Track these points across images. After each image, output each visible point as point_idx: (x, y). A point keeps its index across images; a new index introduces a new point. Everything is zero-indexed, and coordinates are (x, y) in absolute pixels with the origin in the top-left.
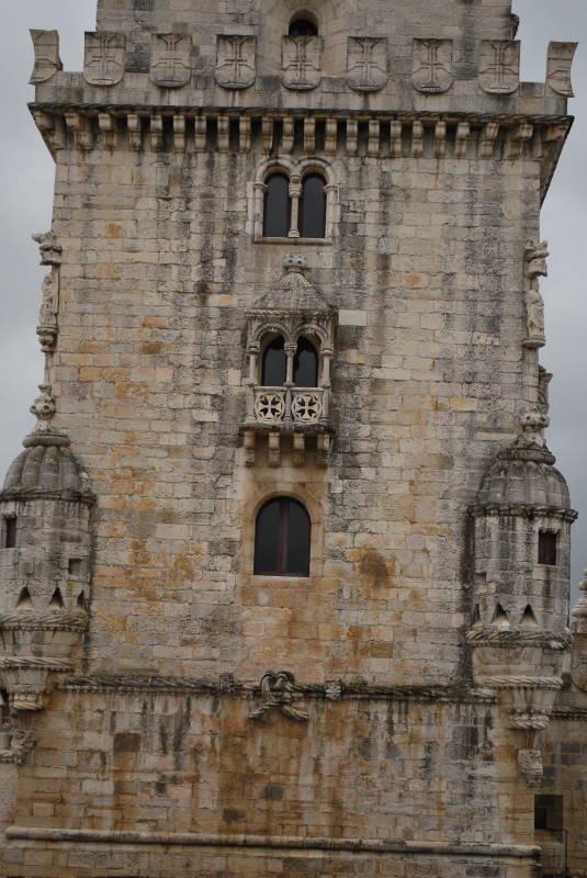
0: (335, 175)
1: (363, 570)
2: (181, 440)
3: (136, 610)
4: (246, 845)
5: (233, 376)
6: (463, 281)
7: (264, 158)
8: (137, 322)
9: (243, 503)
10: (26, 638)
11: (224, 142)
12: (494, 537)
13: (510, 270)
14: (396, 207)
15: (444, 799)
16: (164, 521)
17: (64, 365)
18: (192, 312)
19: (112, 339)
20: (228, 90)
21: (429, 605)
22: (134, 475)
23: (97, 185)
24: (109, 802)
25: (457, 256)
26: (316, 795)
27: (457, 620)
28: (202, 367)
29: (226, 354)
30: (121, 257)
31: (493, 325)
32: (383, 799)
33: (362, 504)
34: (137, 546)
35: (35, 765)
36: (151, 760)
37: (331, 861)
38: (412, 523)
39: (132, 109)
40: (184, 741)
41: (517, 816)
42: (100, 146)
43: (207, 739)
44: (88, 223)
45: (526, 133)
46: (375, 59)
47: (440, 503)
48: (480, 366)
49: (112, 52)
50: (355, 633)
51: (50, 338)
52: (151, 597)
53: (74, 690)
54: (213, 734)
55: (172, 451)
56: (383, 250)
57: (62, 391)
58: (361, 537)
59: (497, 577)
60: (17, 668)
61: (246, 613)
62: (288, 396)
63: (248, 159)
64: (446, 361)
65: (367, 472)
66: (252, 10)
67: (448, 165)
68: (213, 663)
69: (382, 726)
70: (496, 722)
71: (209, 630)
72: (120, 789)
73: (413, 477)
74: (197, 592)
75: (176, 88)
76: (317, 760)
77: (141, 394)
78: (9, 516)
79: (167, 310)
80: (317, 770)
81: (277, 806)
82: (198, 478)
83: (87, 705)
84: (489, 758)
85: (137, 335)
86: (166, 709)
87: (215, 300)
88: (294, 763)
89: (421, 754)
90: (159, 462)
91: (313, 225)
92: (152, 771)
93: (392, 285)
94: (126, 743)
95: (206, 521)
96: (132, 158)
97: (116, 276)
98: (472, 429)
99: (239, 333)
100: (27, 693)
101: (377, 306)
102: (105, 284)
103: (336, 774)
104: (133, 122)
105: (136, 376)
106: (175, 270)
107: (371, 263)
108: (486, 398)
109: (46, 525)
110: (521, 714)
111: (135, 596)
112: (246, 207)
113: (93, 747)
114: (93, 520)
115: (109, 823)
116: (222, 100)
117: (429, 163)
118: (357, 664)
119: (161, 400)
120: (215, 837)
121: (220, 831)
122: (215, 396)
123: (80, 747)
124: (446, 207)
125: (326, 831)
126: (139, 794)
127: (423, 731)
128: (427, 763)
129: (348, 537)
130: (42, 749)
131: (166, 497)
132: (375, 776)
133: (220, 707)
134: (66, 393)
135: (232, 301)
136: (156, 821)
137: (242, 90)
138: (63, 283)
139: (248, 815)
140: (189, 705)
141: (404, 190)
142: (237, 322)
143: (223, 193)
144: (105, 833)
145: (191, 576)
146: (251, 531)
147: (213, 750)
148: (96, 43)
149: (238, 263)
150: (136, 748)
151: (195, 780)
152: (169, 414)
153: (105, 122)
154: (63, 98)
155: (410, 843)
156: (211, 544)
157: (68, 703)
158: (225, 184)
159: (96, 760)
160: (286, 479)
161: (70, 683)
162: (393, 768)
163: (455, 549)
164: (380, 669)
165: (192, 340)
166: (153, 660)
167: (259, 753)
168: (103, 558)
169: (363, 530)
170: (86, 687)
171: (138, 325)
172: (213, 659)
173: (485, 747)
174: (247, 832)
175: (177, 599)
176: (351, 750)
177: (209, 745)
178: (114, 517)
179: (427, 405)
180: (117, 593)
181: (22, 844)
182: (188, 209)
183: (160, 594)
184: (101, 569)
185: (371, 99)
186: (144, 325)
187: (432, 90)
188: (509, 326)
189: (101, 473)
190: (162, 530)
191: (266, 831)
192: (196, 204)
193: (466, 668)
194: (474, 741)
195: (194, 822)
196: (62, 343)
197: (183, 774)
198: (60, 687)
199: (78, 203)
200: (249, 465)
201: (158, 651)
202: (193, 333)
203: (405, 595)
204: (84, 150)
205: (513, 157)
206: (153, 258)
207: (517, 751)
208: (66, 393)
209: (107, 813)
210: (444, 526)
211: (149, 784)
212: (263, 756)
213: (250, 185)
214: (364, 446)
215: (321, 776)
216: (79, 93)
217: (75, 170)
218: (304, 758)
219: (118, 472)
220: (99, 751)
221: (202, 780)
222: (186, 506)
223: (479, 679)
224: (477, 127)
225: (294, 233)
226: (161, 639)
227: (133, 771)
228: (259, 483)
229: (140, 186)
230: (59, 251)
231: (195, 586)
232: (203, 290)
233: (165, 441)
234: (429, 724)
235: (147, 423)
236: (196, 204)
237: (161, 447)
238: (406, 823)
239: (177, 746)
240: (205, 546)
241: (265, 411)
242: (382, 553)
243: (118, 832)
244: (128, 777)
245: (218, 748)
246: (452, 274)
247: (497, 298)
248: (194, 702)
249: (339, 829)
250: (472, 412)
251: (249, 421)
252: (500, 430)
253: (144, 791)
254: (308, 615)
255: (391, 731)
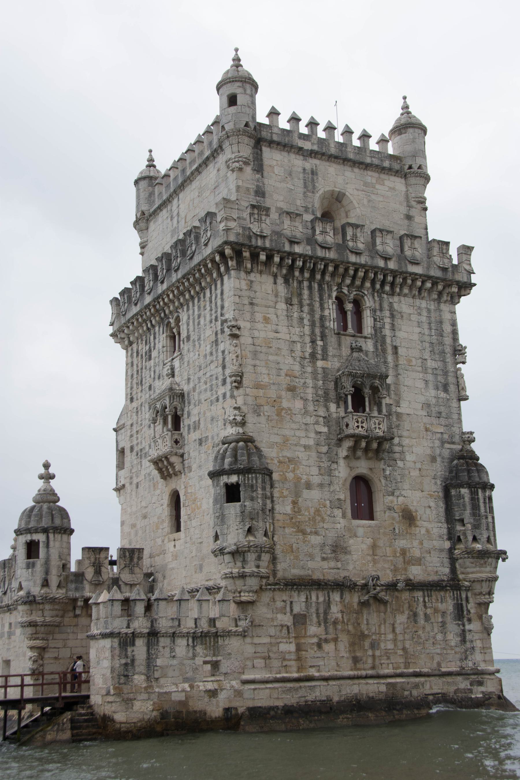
0: (369, 302)
1: (403, 516)
2: (311, 442)
3: (297, 540)
4: (366, 677)
5: (333, 407)
6: (431, 364)
7: (335, 288)
8: (283, 373)
9: (344, 479)
10: (251, 557)
11: (318, 277)
12: (467, 499)
13: (449, 359)
14: (398, 322)
15: (453, 644)
16: (307, 489)
17: (248, 395)
18: (309, 369)
19: (271, 382)
20: (322, 247)
21: (434, 536)
22: (289, 461)
23: (255, 292)
24: (293, 657)
25: (427, 351)
26: (395, 645)
27: (447, 545)
28: (317, 401)
29: (328, 395)
30: (272, 335)
31: (445, 388)
32: (427, 646)
33: (399, 481)
34: (294, 503)
35: (253, 637)
36: (313, 629)
37: (408, 683)
38: (422, 491)
39: (279, 252)
40: (329, 617)
41: (486, 651)
42: (255, 270)
43: (339, 615)
44: (253, 313)
45: (455, 289)
46: (388, 241)
47: (433, 481)
48: (442, 409)
49: (264, 218)
50: (404, 552)
51: (239, 378)
52: (304, 533)
53: (270, 589)
54: (342, 612)
55: (306, 447)
56: (394, 344)
57: (248, 411)
58: (401, 499)
59: (472, 521)
60: (246, 576)
61: (351, 541)
62: (368, 419)
63: (328, 287)
64: (427, 405)
65: (400, 464)
66: (313, 206)
67: (418, 302)
68: (338, 571)
69: (421, 604)
70: (471, 600)
71: (334, 551)
72: (299, 648)
73: (420, 467)
74: (327, 529)
75: (298, 243)
76: (393, 625)
77: (288, 414)
78: (232, 484)
79: (297, 367)
80: (394, 631)
81: (377, 653)
82: (322, 465)
83: (277, 598)
84: (470, 620)
85: (284, 381)
86: (318, 598)
87: (320, 364)
88: (383, 626)
89: (440, 620)
90: (302, 454)
91: (359, 328)
92: (314, 636)
93: (400, 363)
94: (300, 620)
95: (327, 489)
96: (271, 279)
97: (270, 345)
98: (443, 442)
99: (333, 383)
100: (249, 592)
101: (395, 373)
102: (264, 350)
103: (403, 632)
104: (277, 259)
105: (285, 404)
106: (299, 345)
107: (389, 350)
108: (446, 426)
109: (259, 489)
110: (484, 595)
111: (296, 532)
112: (330, 314)
113: (283, 623)
114: (272, 486)
115: (295, 669)
116: (320, 253)
117: (411, 300)
118: (406, 569)
119: (298, 418)
120: (351, 673)
121: (352, 670)
122: (324, 418)
123: (275, 624)
124: (419, 324)
125: (402, 665)
126: (309, 650)
127: (441, 607)
128: (443, 624)
129: (395, 499)
130: (255, 626)
131: (306, 474)
132: (420, 632)
133: (344, 596)
134: (250, 412)
135: (328, 365)
136: (319, 666)
137: (329, 249)
138: (243, 348)
139: (364, 659)
140: (329, 596)
141: (400, 313)
142: (331, 377)
143: (317, 305)
144: (295, 675)
145: (323, 520)
146: (348, 494)
147: (343, 622)
148: (256, 211)
149: (329, 344)
150: (304, 623)
151: (336, 640)
152: (303, 427)
153: (263, 257)
154: (241, 240)
155: (443, 670)
156: (331, 502)
157: (266, 597)
158: (318, 299)
159: (285, 631)
160: (362, 467)
161: (269, 585)
162: (428, 628)
163: (442, 505)
164: (415, 572)
165: (311, 385)
166: (308, 570)
167: (365, 623)
168: (277, 509)
169: (402, 495)
170: (277, 587)
171: (283, 375)
172: (338, 569)
173: (467, 614)
174: (364, 670)
175: (316, 533)
176: (408, 618)
177: (341, 619)
178: (281, 485)
179: (422, 428)
180: (287, 530)
181: (253, 686)
182: (302, 311)
183: (309, 530)
184: (277, 516)
185: (388, 262)
186: (286, 375)
187: (416, 262)
188: (452, 388)
189: (272, 460)
190: (306, 493)
191: (373, 668)
192: (306, 309)
193: (453, 570)
194: (463, 612)
195: (338, 665)
196: (245, 382)
197: (329, 637)
198: (263, 587)
199: (246, 302)
200: (346, 458)
201: (310, 564)
202: (311, 381)
203: (423, 531)
204: (248, 273)
205: (445, 302)
206: (287, 337)
207: (481, 616)
208: (250, 412)
209: (293, 663)
210: (436, 493)
211: (313, 644)
212: (367, 624)
213: (330, 301)
214: (397, 449)
215: (396, 633)
216: (250, 238)
217: (243, 283)
218: (387, 625)
219: (281, 458)
220: (286, 625)
221: (339, 640)
222: (316, 480)
223: (461, 577)
224: (435, 284)
225: (350, 330)
226: (312, 557)
227: (304, 637)
228: (351, 467)
229: (276, 296)
230: (239, 329)
231: (326, 526)
232: (313, 356)
233: (303, 442)
234: (442, 602)
235: (293, 432)
236: (306, 309)
237: (301, 445)
238: (437, 659)
239: (326, 621)
240: (328, 502)
241: (358, 427)
242: (411, 508)
243: (302, 674)
244: (303, 641)
245: (346, 621)
246: (426, 360)
247: (446, 373)
248: (331, 593)
249: (407, 664)
250: (442, 433)
251: (350, 431)
252: (453, 443)
253: (312, 649)
254: (381, 543)
255: (425, 606)
